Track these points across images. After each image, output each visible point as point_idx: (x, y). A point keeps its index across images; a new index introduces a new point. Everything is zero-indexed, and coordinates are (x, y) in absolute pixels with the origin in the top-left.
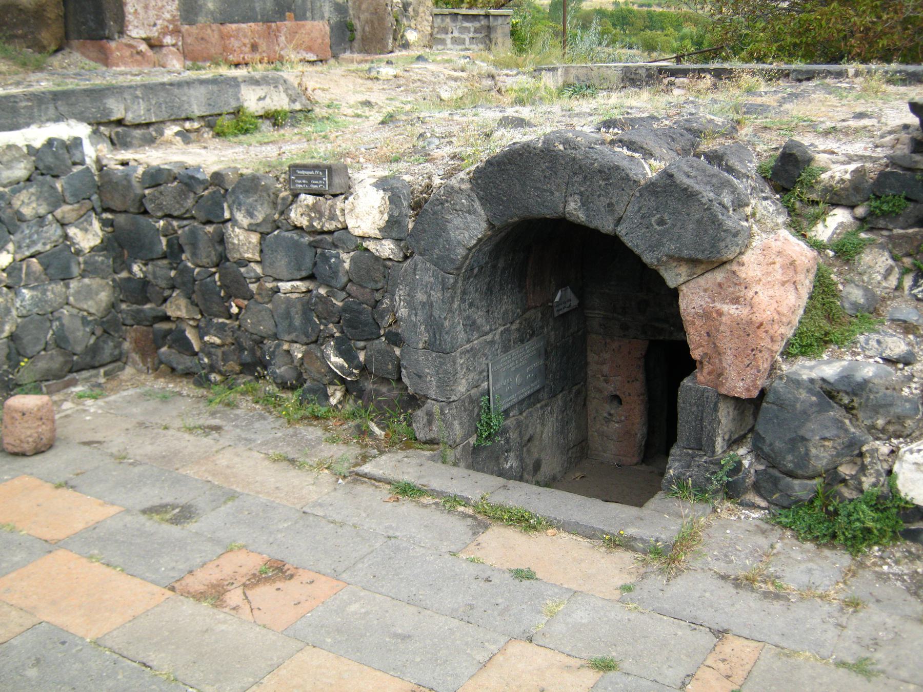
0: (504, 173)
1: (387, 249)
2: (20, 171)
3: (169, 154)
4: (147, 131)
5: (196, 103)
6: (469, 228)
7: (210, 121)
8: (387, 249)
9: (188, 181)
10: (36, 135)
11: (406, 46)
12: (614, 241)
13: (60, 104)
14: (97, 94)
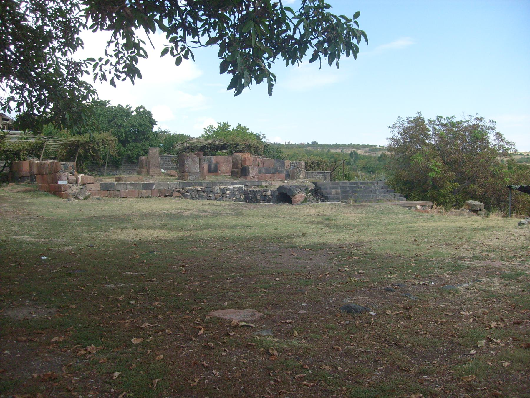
0: (280, 188)
1: (271, 197)
2: (237, 189)
3: (253, 189)
4: (250, 187)
5: (256, 184)
6: (277, 194)
7: (258, 186)
8: (271, 197)
9: (253, 191)
10: (239, 186)
11: (299, 178)
12: (286, 194)
13: (241, 183)
14: (245, 182)
